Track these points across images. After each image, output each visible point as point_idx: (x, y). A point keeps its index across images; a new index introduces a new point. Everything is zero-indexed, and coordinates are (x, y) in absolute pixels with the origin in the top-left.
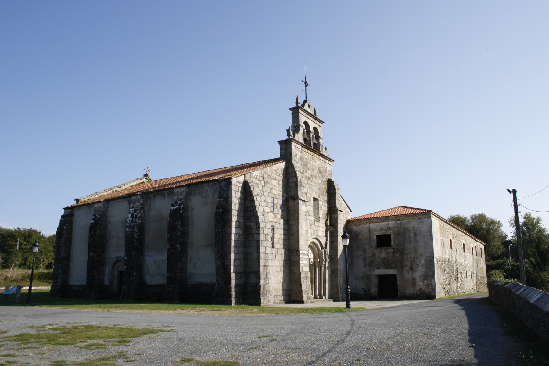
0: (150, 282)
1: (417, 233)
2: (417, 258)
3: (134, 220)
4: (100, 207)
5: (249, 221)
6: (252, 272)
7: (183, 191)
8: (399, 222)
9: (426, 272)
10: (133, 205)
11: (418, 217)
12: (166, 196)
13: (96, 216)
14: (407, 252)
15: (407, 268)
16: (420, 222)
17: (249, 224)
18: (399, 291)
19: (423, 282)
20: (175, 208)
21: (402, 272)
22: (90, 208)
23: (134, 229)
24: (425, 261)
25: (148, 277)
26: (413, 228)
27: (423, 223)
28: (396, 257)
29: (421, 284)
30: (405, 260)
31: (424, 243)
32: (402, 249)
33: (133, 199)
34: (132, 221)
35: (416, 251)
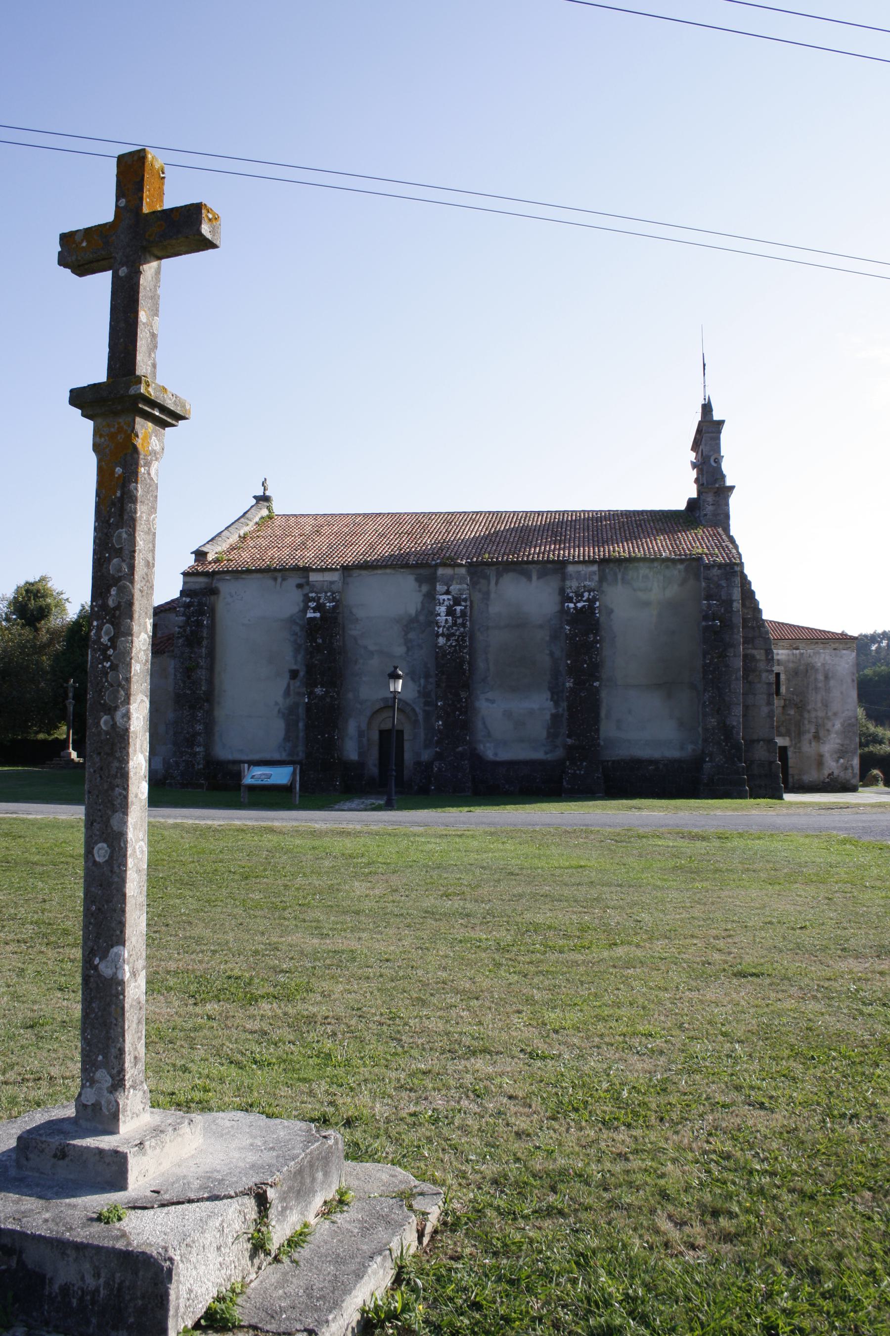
0: (496, 754)
1: (830, 675)
2: (828, 718)
3: (460, 621)
4: (332, 583)
5: (750, 646)
6: (758, 741)
7: (594, 573)
8: (798, 651)
9: (842, 745)
10: (446, 588)
11: (833, 646)
12: (534, 577)
13: (321, 601)
14: (809, 707)
15: (809, 736)
16: (836, 656)
17: (749, 651)
18: (790, 777)
19: (837, 761)
20: (579, 605)
21: (800, 742)
22: (279, 580)
23: (464, 641)
24: (842, 725)
25: (488, 745)
26: (823, 665)
27: (841, 657)
28: (789, 715)
29: (834, 764)
30: (806, 722)
31: (842, 693)
32: (801, 701)
33: (443, 575)
34: (455, 624)
35: (827, 706)
